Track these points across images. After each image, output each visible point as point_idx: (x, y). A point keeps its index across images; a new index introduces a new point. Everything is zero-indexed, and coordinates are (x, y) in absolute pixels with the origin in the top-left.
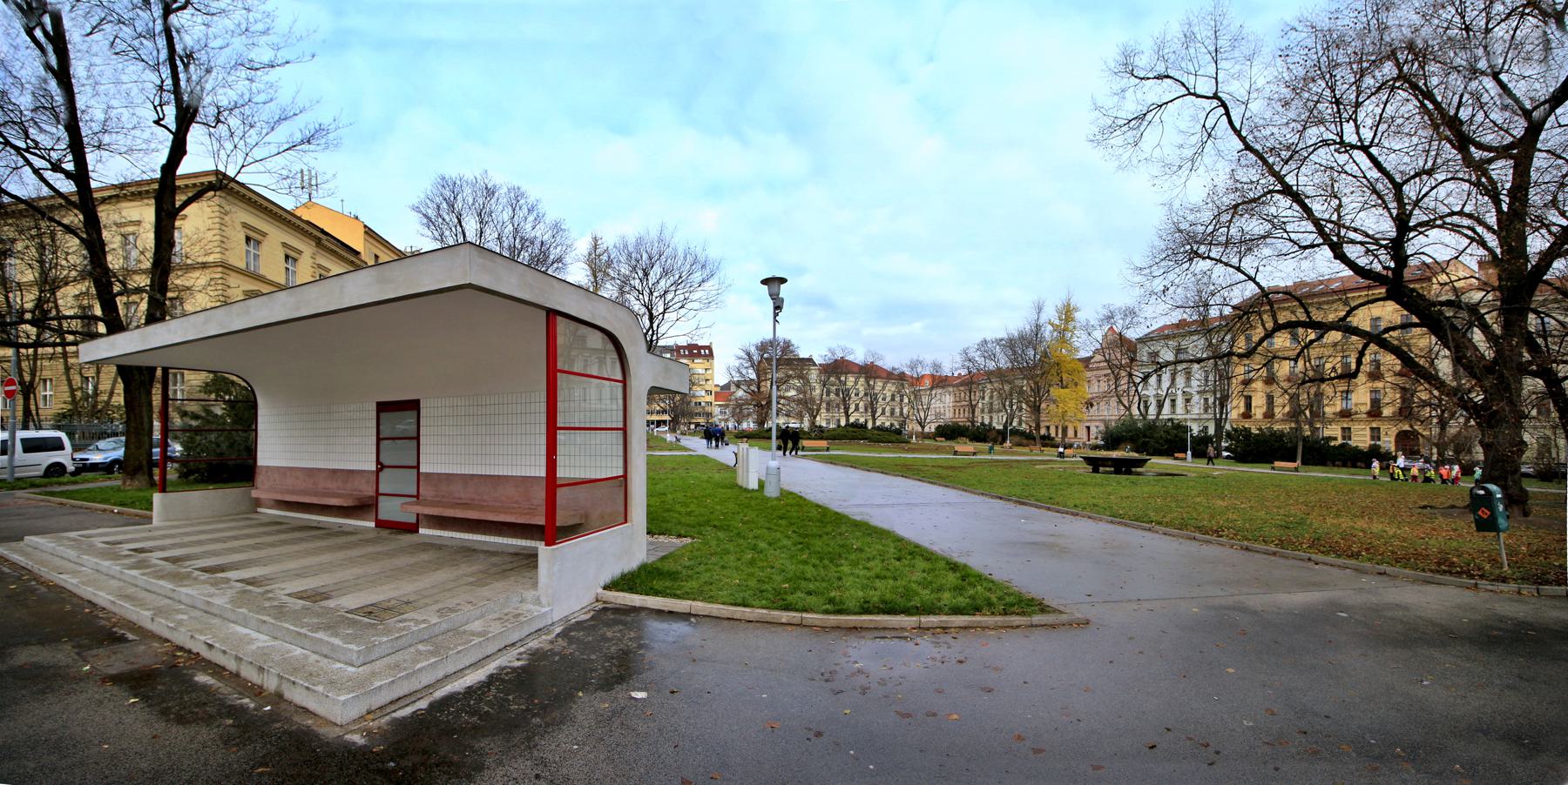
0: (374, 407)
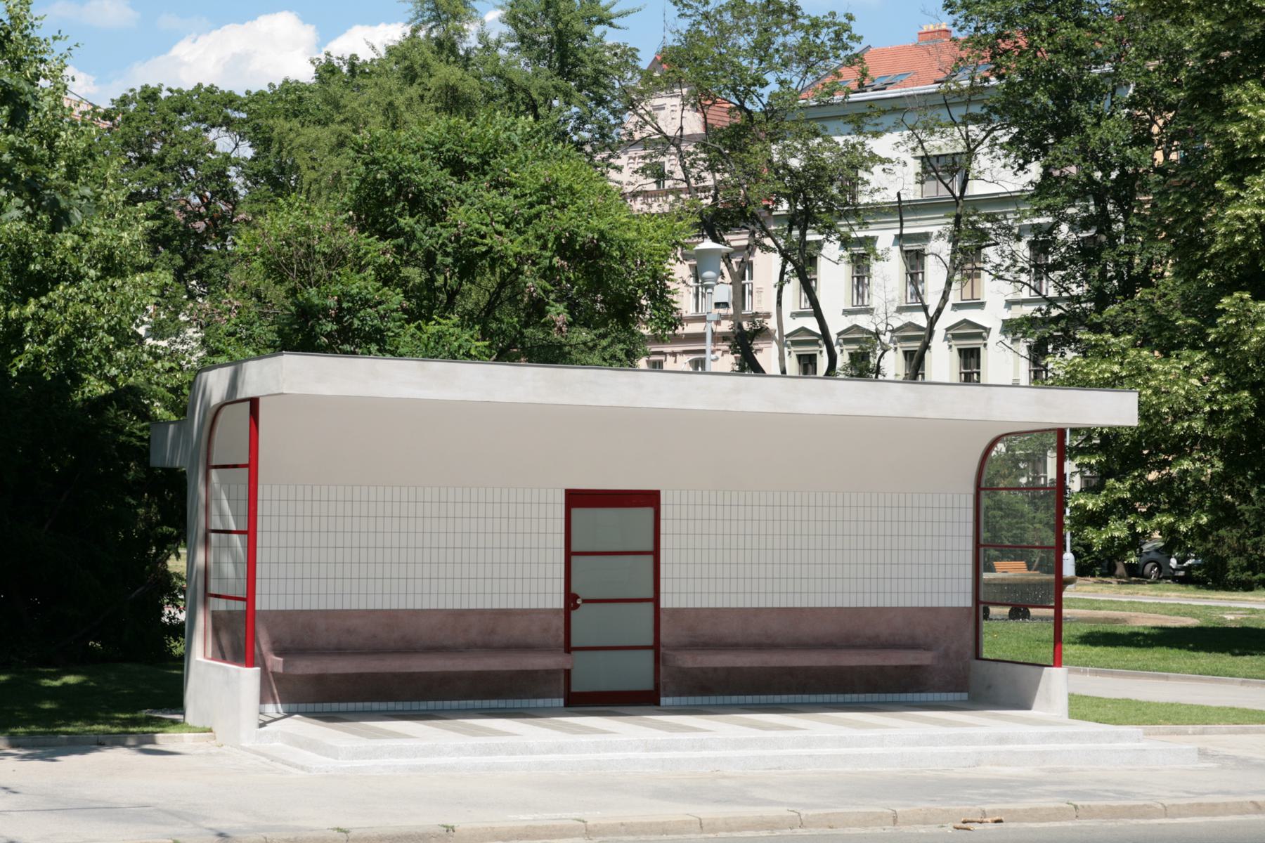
0: (561, 499)
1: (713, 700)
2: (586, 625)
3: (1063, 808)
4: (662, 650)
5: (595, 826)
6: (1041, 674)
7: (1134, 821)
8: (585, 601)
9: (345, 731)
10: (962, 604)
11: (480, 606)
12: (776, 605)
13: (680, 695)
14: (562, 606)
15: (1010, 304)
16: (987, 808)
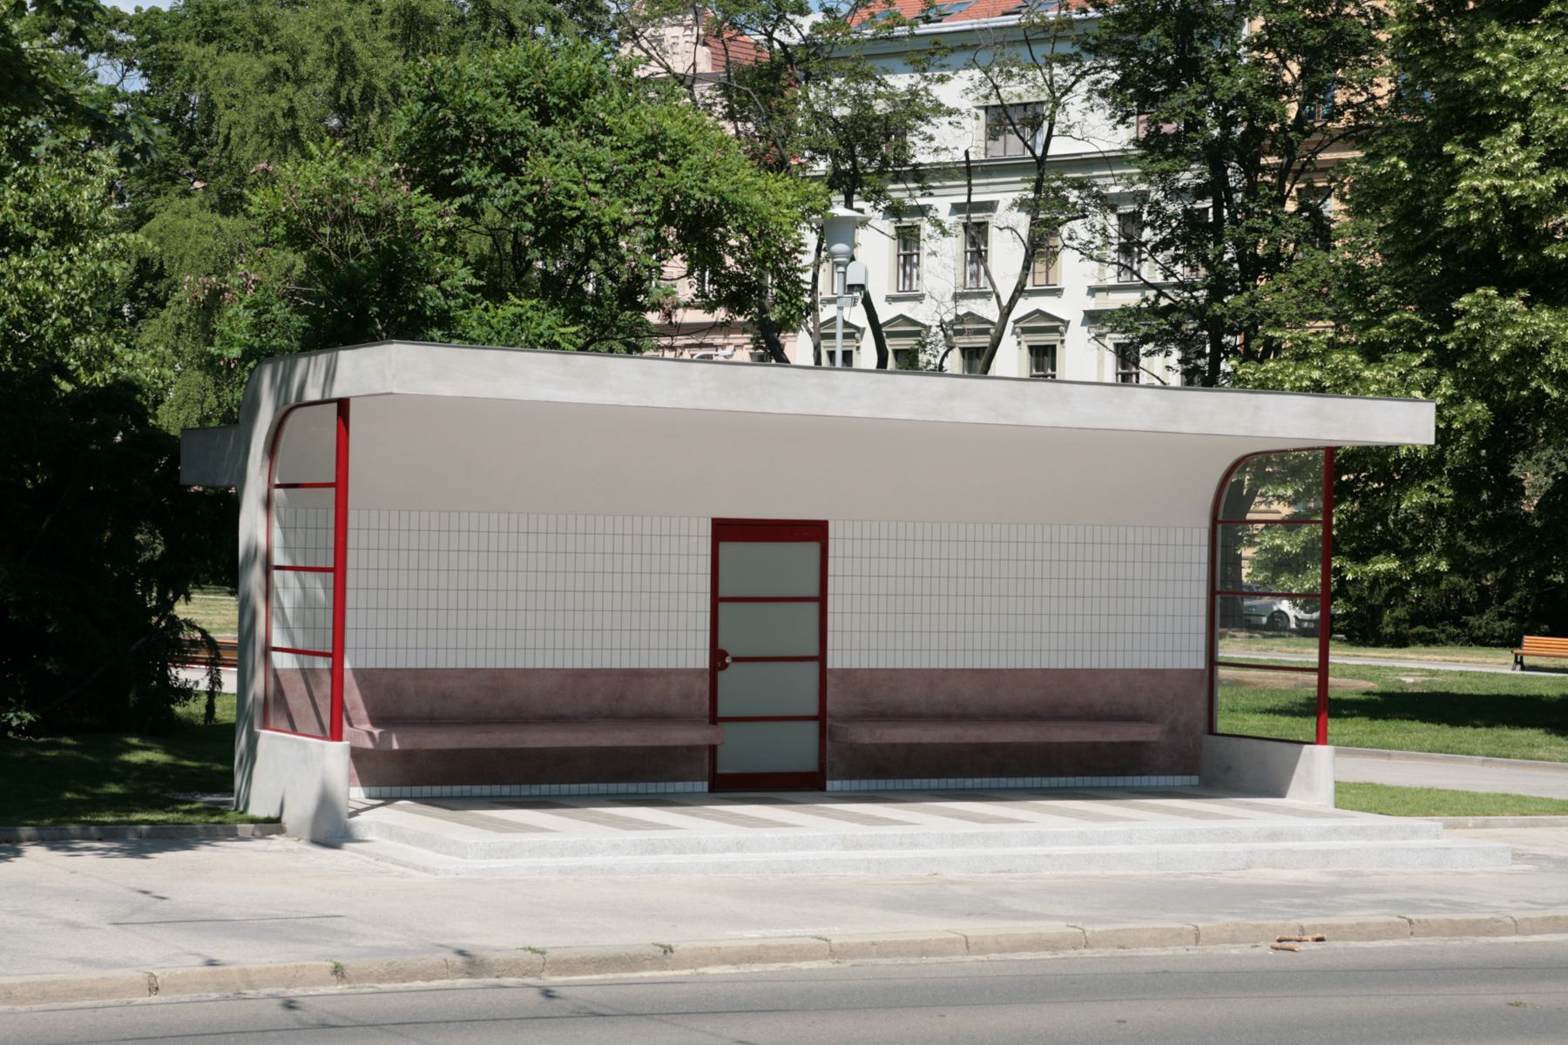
0: (706, 530)
1: (890, 784)
2: (738, 688)
3: (1396, 924)
4: (829, 721)
5: (841, 945)
6: (1299, 753)
7: (1482, 940)
8: (735, 660)
9: (461, 823)
10: (1193, 666)
11: (606, 665)
12: (969, 666)
13: (851, 777)
14: (707, 666)
15: (1093, 291)
16: (1306, 922)
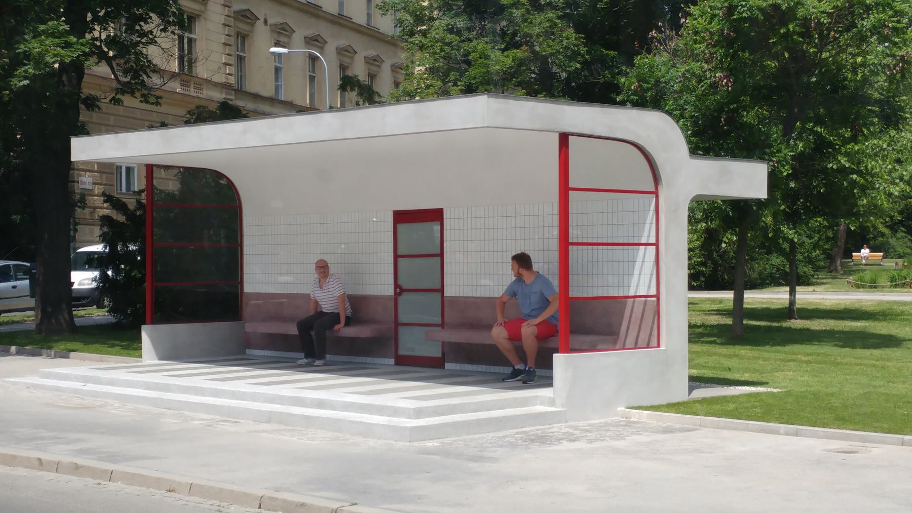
14: (393, 294)
